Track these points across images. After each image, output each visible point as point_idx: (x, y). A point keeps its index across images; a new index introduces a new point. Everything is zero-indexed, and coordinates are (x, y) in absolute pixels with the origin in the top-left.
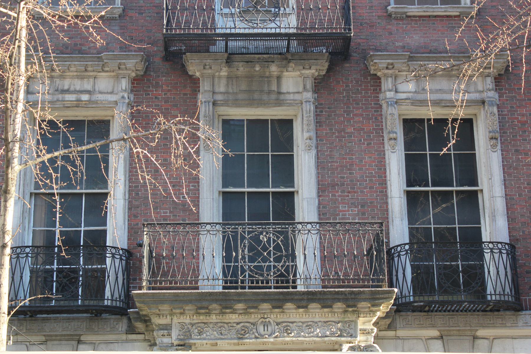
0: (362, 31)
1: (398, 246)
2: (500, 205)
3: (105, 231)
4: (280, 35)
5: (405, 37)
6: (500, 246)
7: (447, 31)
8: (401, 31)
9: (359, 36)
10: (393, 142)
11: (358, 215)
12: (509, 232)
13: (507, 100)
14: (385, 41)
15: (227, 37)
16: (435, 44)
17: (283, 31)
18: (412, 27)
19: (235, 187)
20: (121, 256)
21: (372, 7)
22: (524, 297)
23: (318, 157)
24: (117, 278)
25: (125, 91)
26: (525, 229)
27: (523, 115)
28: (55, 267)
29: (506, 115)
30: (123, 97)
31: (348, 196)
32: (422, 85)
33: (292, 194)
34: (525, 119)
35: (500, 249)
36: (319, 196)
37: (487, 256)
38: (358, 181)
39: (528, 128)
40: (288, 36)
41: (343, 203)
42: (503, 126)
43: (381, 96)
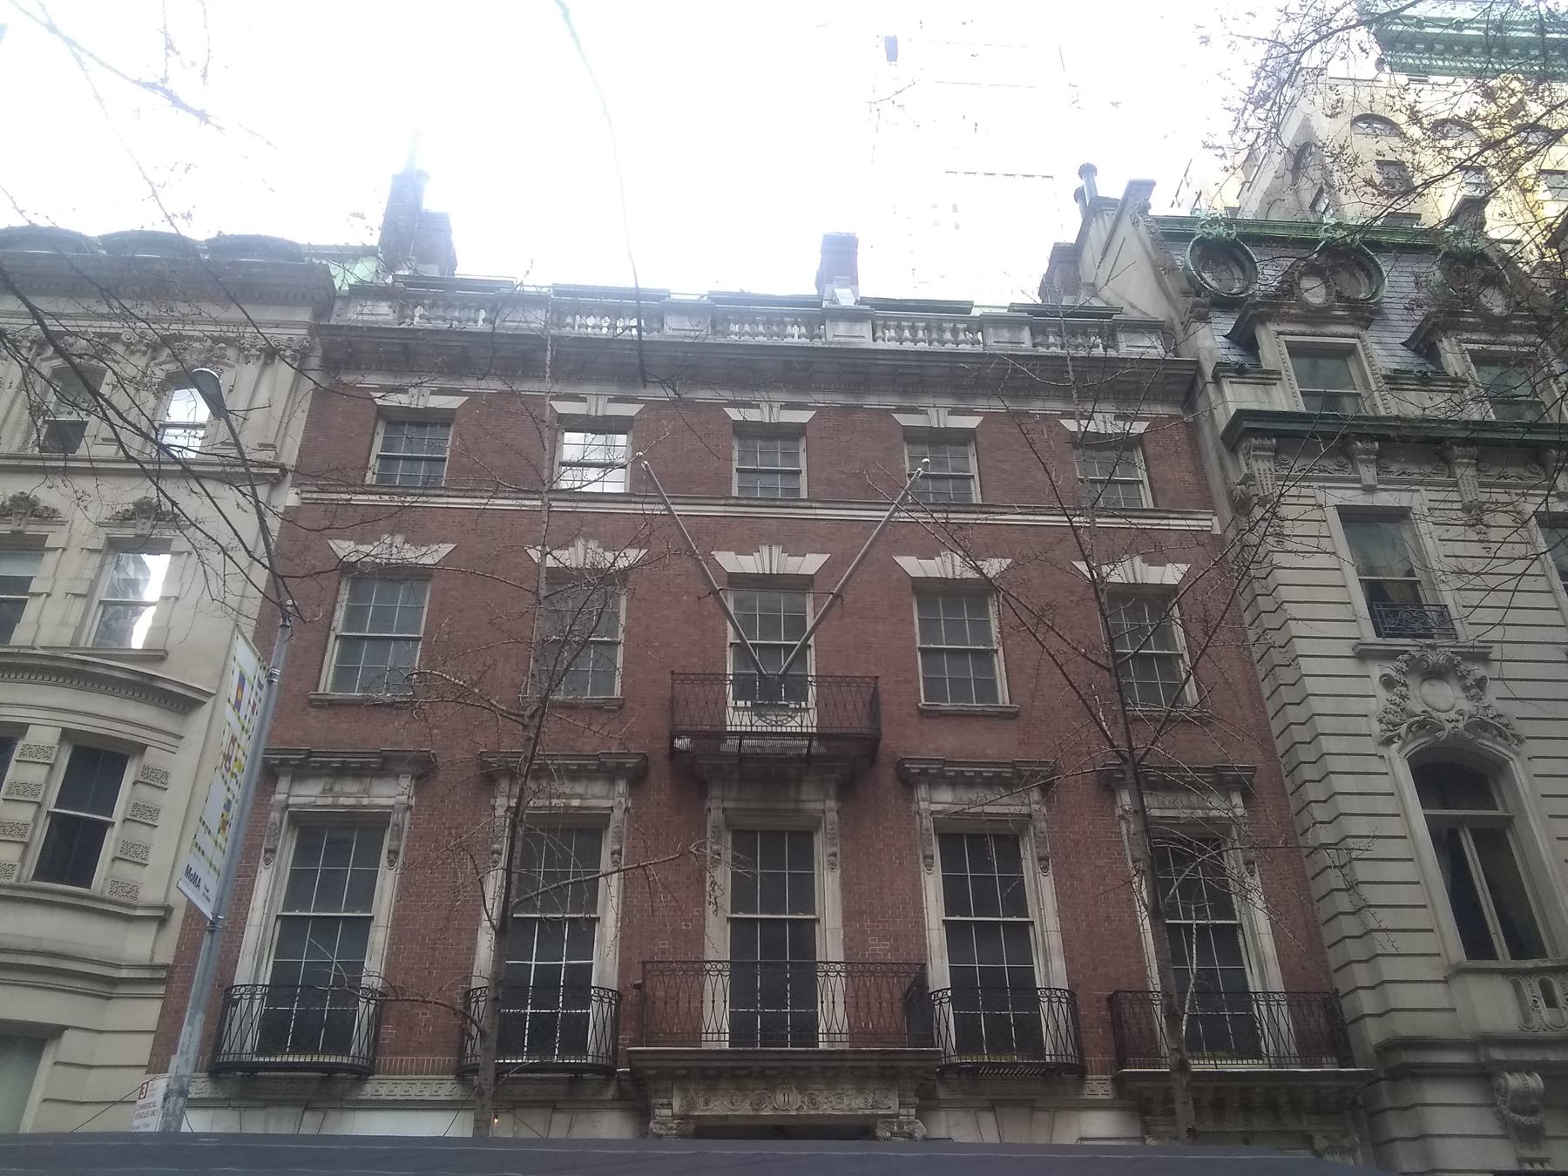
1: (939, 991)
2: (1055, 941)
3: (591, 965)
4: (801, 734)
6: (1059, 994)
10: (929, 860)
11: (889, 950)
15: (742, 735)
17: (805, 730)
19: (745, 913)
20: (611, 999)
23: (842, 878)
24: (605, 1027)
25: (622, 796)
27: (1076, 833)
28: (529, 1011)
30: (620, 802)
31: (878, 927)
33: (813, 922)
34: (1078, 837)
35: (1059, 998)
36: (844, 926)
37: (1044, 1006)
40: (810, 736)
43: (914, 807)
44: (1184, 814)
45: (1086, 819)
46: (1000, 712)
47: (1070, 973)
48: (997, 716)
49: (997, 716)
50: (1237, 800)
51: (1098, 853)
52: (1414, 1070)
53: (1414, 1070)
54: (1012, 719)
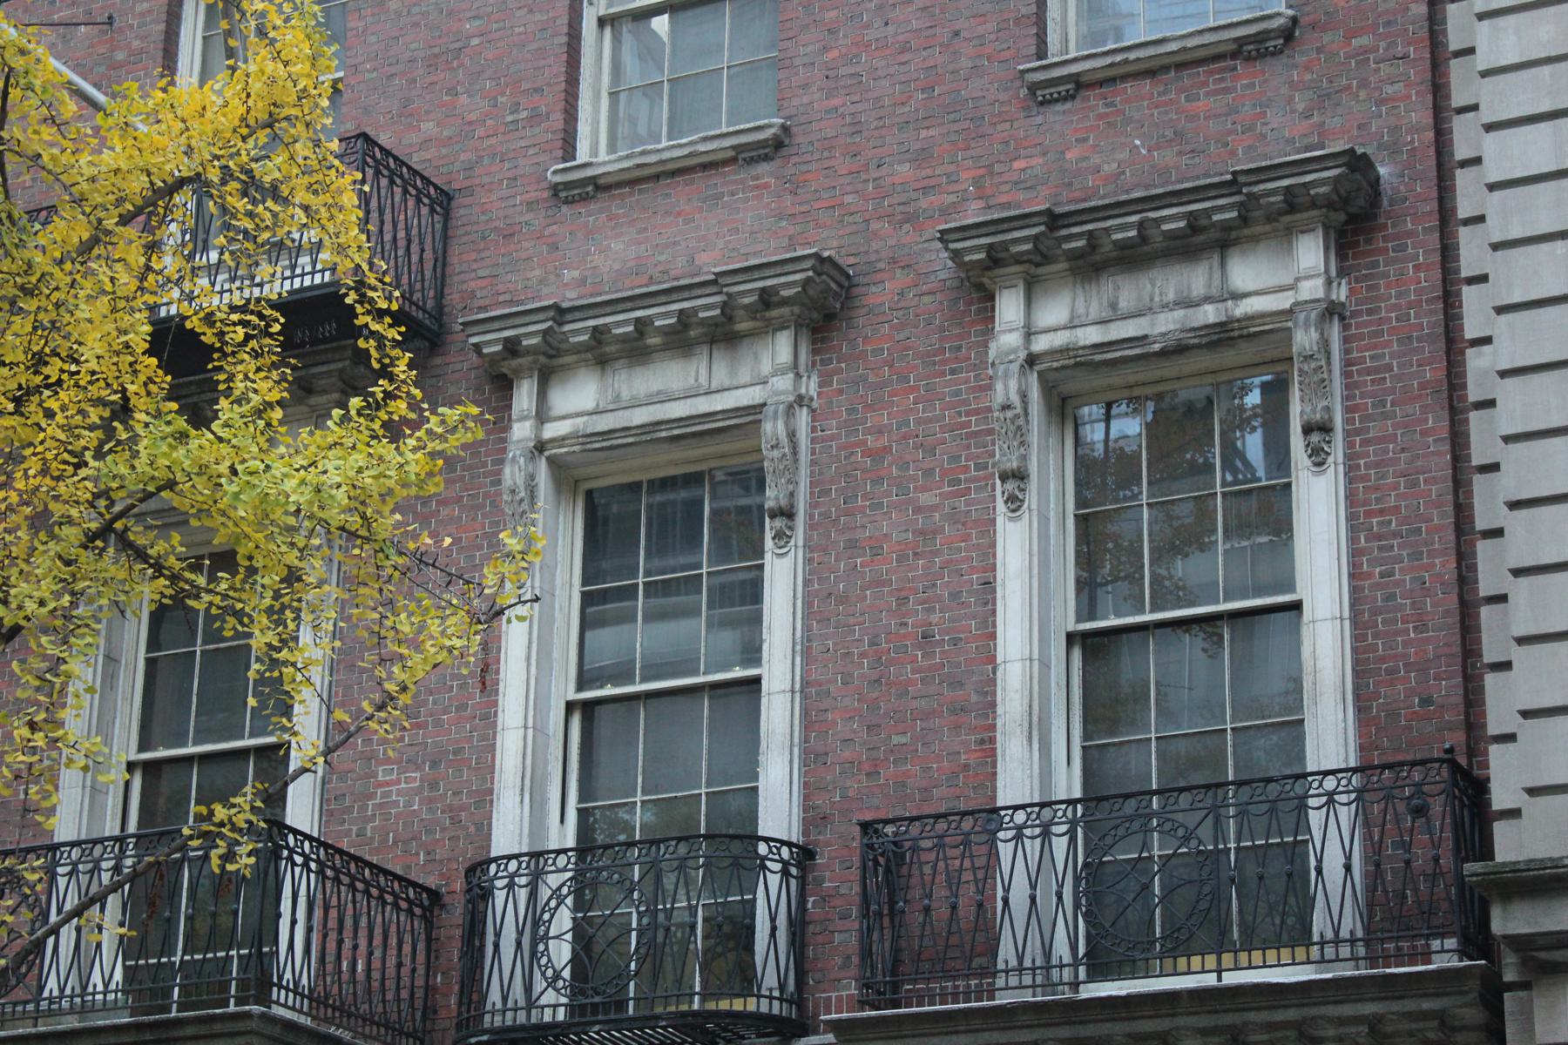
0: (483, 255)
5: (588, 252)
7: (701, 209)
8: (580, 235)
9: (475, 270)
11: (420, 790)
12: (806, 797)
13: (840, 392)
14: (537, 272)
16: (663, 258)
21: (515, 179)
22: (824, 991)
26: (849, 783)
27: (880, 431)
29: (832, 438)
32: (616, 385)
34: (884, 441)
38: (431, 693)
39: (890, 466)
41: (388, 761)
42: (821, 474)
44: (1165, 324)
45: (912, 389)
46: (737, 148)
47: (809, 791)
48: (734, 160)
49: (732, 161)
50: (1310, 253)
51: (929, 472)
52: (1543, 955)
53: (1543, 955)
54: (766, 158)
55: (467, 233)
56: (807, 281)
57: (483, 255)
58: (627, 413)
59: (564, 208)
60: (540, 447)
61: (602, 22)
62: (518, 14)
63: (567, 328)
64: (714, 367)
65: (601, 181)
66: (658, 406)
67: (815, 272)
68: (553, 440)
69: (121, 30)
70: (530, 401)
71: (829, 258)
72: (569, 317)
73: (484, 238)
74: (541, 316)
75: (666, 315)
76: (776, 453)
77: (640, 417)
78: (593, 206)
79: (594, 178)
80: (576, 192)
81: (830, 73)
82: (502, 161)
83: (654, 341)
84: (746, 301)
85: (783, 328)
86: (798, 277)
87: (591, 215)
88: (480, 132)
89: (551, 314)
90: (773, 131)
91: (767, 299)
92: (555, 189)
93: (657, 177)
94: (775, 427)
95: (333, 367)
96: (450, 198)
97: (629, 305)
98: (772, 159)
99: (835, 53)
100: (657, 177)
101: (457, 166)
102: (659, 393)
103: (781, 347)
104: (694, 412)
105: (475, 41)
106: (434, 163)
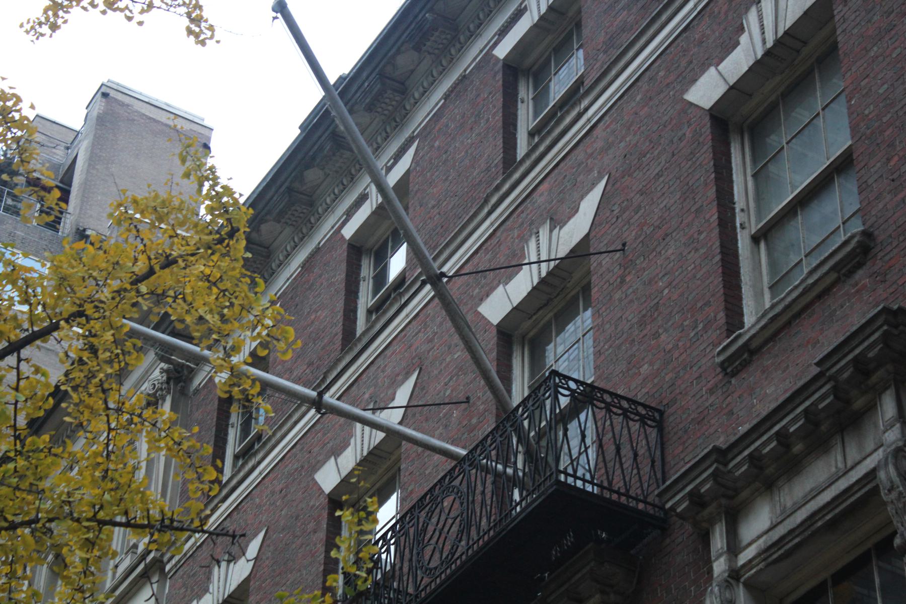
5: (753, 406)
9: (683, 459)
18: (763, 372)
32: (782, 500)
54: (860, 265)
55: (676, 433)
56: (885, 334)
57: (687, 445)
58: (792, 519)
59: (733, 381)
60: (735, 575)
61: (756, 239)
62: (689, 257)
63: (731, 465)
64: (848, 450)
65: (754, 345)
66: (812, 502)
67: (888, 325)
68: (744, 566)
69: (474, 403)
70: (722, 542)
71: (900, 309)
72: (730, 456)
73: (686, 431)
74: (708, 462)
75: (794, 421)
76: (894, 495)
77: (801, 515)
78: (751, 369)
79: (746, 344)
80: (737, 363)
81: (895, 176)
82: (691, 368)
83: (798, 448)
84: (846, 375)
85: (886, 389)
86: (877, 335)
87: (751, 376)
88: (676, 355)
89: (714, 457)
90: (856, 240)
91: (862, 367)
92: (722, 364)
93: (788, 324)
94: (887, 473)
95: (585, 571)
96: (661, 413)
97: (768, 424)
98: (864, 264)
99: (896, 158)
100: (788, 324)
101: (665, 386)
102: (812, 490)
103: (888, 407)
104: (838, 492)
105: (666, 291)
106: (650, 394)
